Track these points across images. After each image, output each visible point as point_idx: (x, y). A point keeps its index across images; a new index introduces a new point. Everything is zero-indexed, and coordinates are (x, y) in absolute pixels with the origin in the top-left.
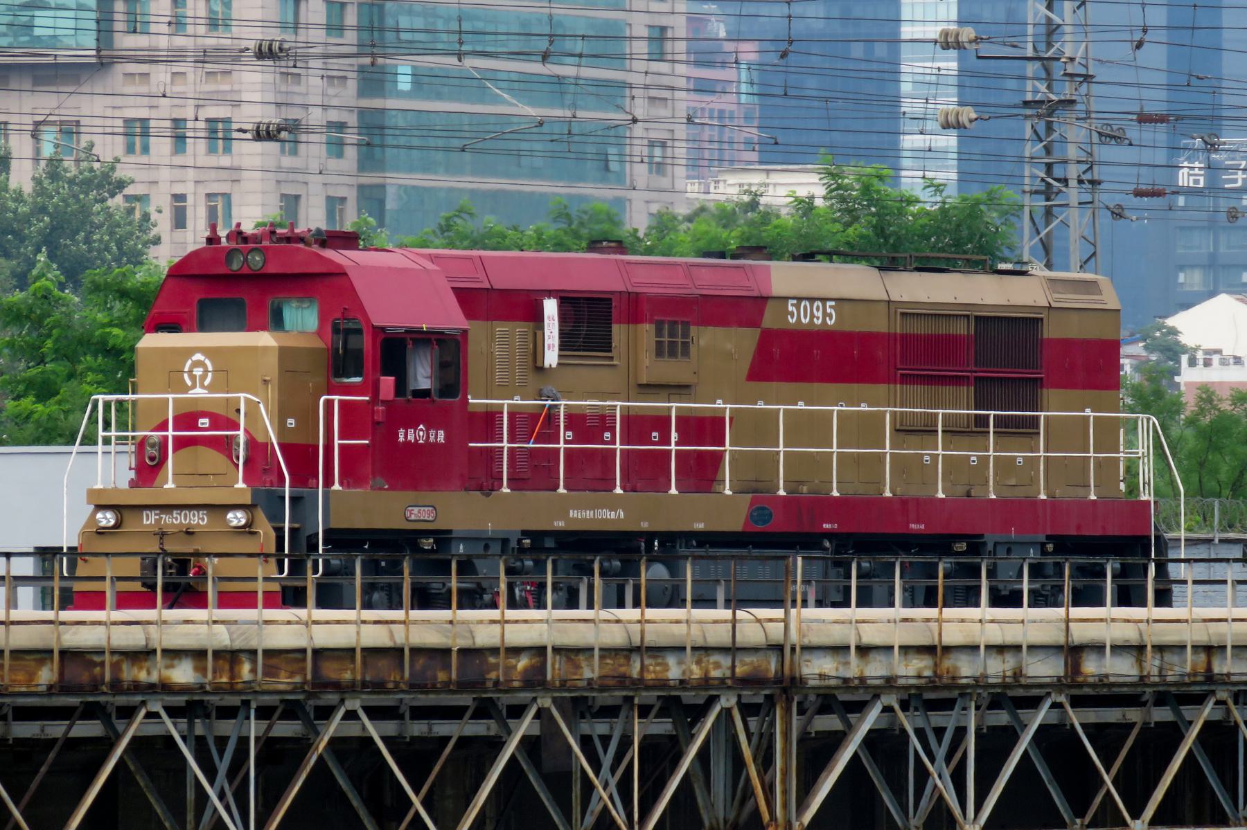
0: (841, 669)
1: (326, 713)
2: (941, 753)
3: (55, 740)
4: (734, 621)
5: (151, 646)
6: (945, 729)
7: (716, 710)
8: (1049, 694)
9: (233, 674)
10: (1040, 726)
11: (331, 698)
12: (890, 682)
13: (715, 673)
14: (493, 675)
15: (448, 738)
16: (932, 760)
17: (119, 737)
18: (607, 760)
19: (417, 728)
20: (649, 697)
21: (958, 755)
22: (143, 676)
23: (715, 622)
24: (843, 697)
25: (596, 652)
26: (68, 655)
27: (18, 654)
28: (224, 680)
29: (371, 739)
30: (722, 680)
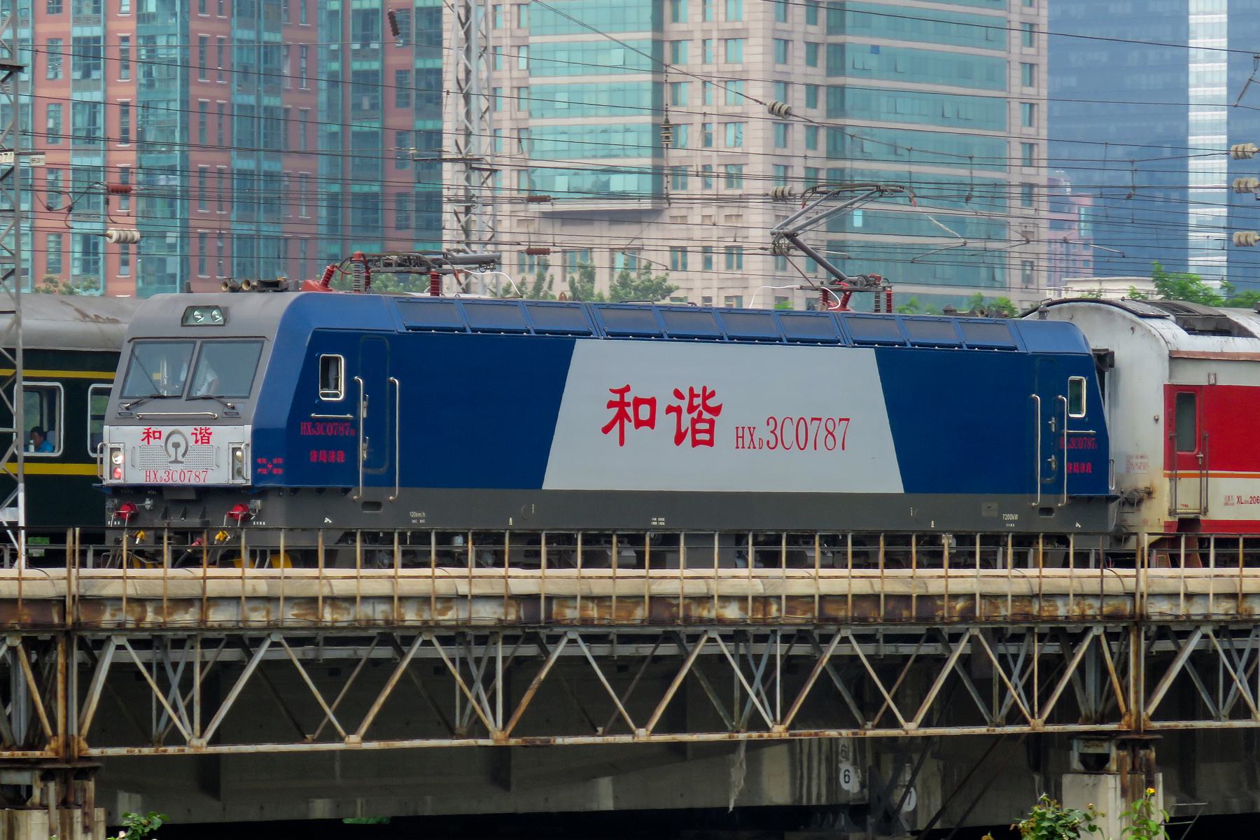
1: (827, 639)
2: (1241, 665)
3: (645, 657)
4: (1102, 577)
5: (711, 593)
9: (766, 613)
11: (831, 628)
12: (1207, 619)
13: (1089, 612)
14: (940, 613)
15: (907, 657)
16: (1235, 671)
17: (688, 655)
18: (1016, 672)
19: (888, 649)
20: (1045, 628)
21: (1253, 667)
22: (705, 614)
24: (1175, 628)
25: (1009, 598)
27: (621, 598)
29: (858, 657)
30: (1094, 617)
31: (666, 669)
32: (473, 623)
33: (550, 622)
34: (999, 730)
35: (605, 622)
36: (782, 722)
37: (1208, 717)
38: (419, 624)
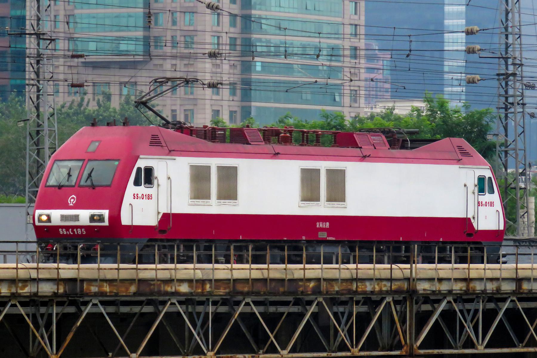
0: (432, 287)
1: (238, 303)
2: (469, 318)
3: (136, 313)
4: (391, 269)
5: (173, 277)
6: (470, 310)
7: (385, 302)
8: (510, 297)
9: (203, 289)
10: (507, 309)
12: (450, 292)
13: (384, 289)
15: (284, 313)
16: (466, 322)
17: (160, 312)
18: (343, 321)
19: (272, 309)
22: (169, 289)
23: (384, 269)
24: (432, 298)
25: (340, 281)
26: (141, 281)
27: (123, 281)
28: (200, 291)
29: (255, 313)
30: (387, 291)
31: (147, 320)
32: (39, 294)
33: (83, 294)
34: (333, 355)
35: (113, 294)
36: (212, 350)
37: (451, 347)
38: (9, 295)
